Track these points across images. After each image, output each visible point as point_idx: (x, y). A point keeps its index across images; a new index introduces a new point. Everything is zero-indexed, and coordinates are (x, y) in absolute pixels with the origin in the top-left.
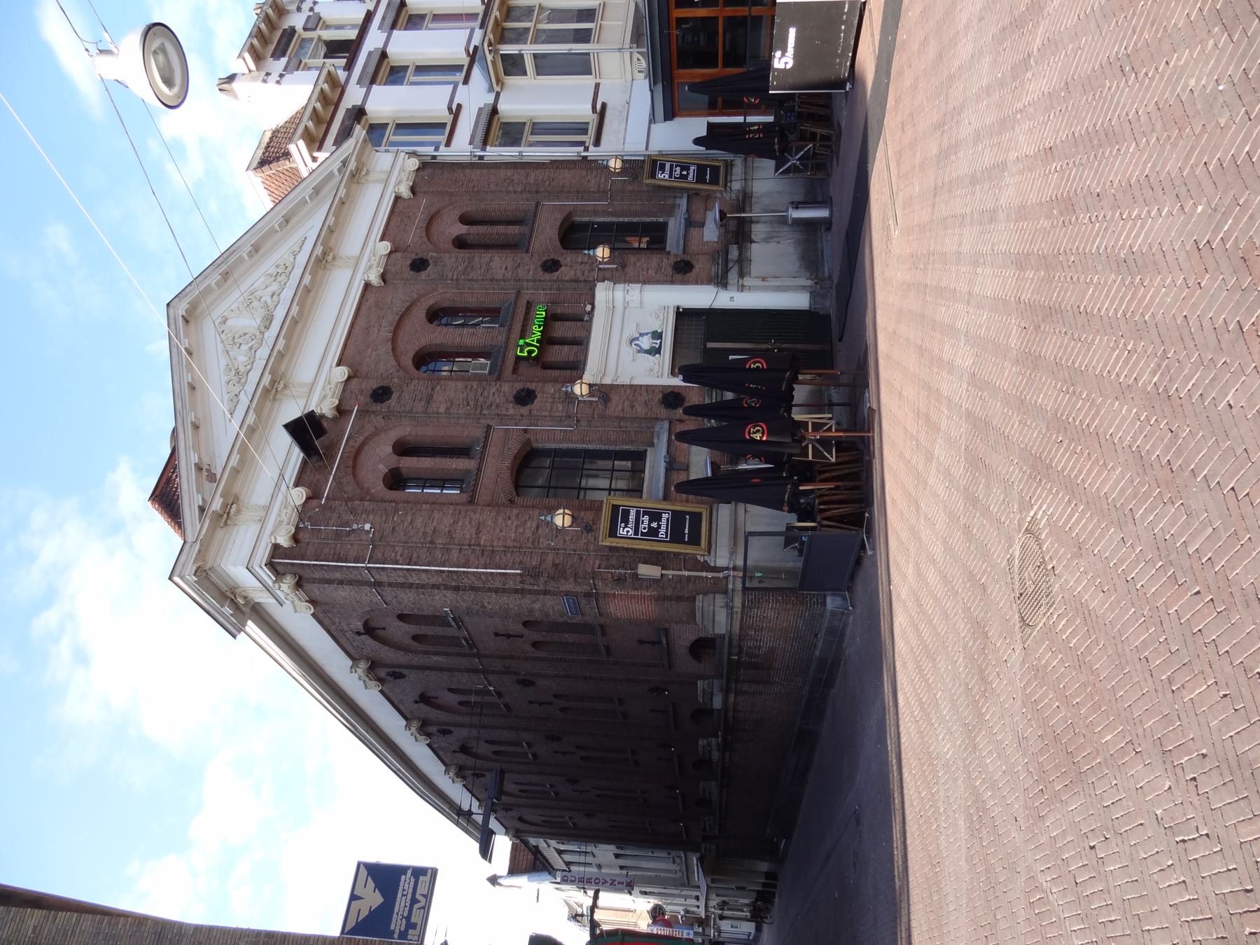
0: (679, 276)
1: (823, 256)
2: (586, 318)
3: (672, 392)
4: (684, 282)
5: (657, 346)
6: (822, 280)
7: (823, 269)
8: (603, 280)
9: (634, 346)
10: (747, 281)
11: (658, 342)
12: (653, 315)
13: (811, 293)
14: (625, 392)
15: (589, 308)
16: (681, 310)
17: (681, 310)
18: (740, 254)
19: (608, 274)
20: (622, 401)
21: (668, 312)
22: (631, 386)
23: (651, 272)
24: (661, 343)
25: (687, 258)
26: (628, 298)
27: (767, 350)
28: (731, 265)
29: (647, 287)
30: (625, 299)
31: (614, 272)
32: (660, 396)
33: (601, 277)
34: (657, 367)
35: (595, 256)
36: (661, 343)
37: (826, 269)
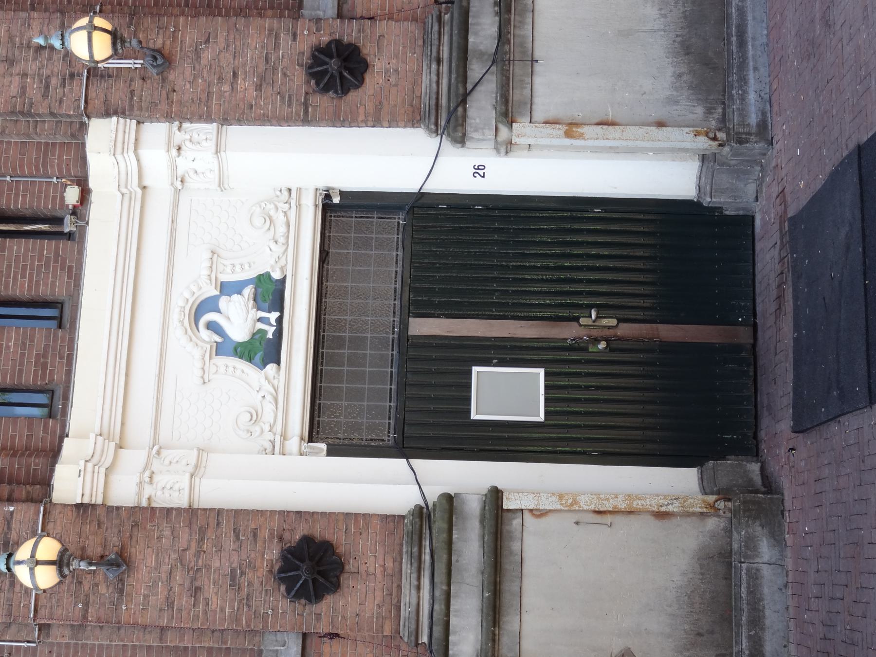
0: (324, 102)
1: (742, 44)
2: (68, 226)
3: (307, 540)
4: (339, 120)
5: (271, 331)
6: (740, 142)
7: (743, 99)
8: (107, 114)
9: (205, 334)
10: (522, 131)
11: (274, 316)
12: (258, 221)
13: (703, 158)
14: (174, 535)
15: (72, 195)
16: (336, 200)
17: (336, 200)
18: (503, 37)
19: (118, 94)
20: (165, 568)
21: (299, 206)
22: (191, 513)
23: (246, 86)
24: (280, 320)
25: (350, 32)
26: (184, 164)
27: (578, 347)
28: (476, 70)
29: (236, 133)
30: (174, 168)
31: (137, 84)
32: (273, 553)
33: (97, 103)
34: (269, 407)
35: (68, 55)
36: (280, 320)
37: (752, 97)
